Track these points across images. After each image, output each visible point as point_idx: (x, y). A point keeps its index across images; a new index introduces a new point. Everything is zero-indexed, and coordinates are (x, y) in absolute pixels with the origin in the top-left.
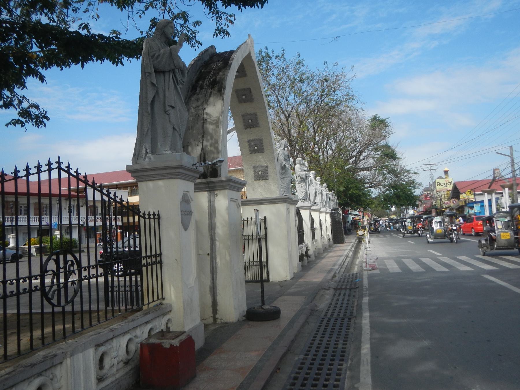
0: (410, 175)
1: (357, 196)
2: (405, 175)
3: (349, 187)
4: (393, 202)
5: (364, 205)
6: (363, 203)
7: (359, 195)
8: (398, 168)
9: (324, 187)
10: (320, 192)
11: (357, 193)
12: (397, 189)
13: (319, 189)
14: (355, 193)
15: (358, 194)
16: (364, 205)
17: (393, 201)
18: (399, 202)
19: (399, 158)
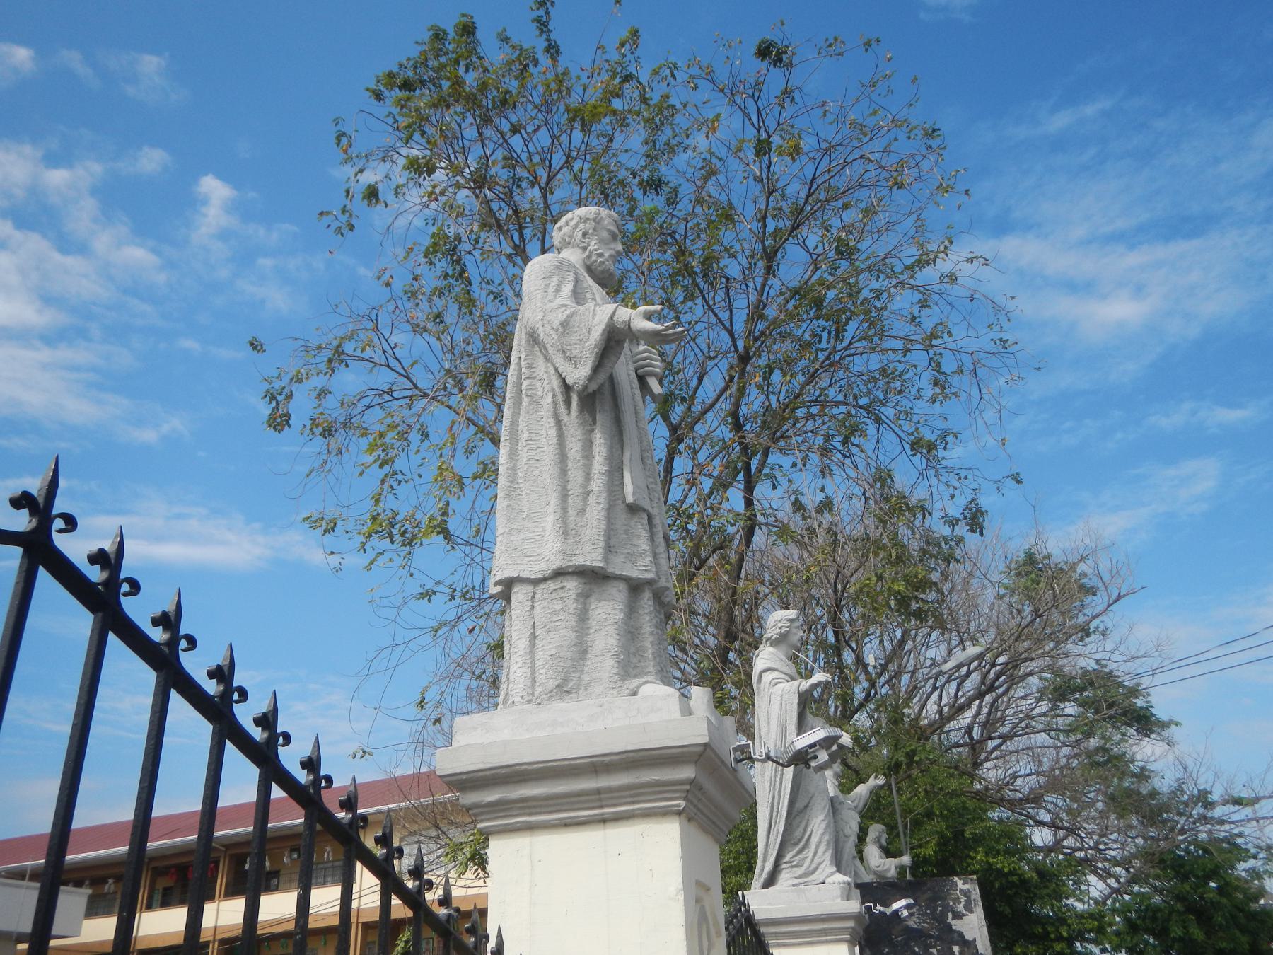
0: (1218, 812)
1: (1013, 885)
2: (1199, 810)
3: (967, 834)
4: (1181, 939)
5: (1060, 938)
6: (1050, 929)
7: (1024, 883)
8: (1164, 783)
9: (776, 642)
10: (578, 374)
11: (1011, 873)
12: (1185, 878)
13: (565, 325)
14: (1000, 872)
15: (1015, 878)
16: (1060, 938)
17: (1177, 931)
18: (1208, 934)
19: (1165, 725)
